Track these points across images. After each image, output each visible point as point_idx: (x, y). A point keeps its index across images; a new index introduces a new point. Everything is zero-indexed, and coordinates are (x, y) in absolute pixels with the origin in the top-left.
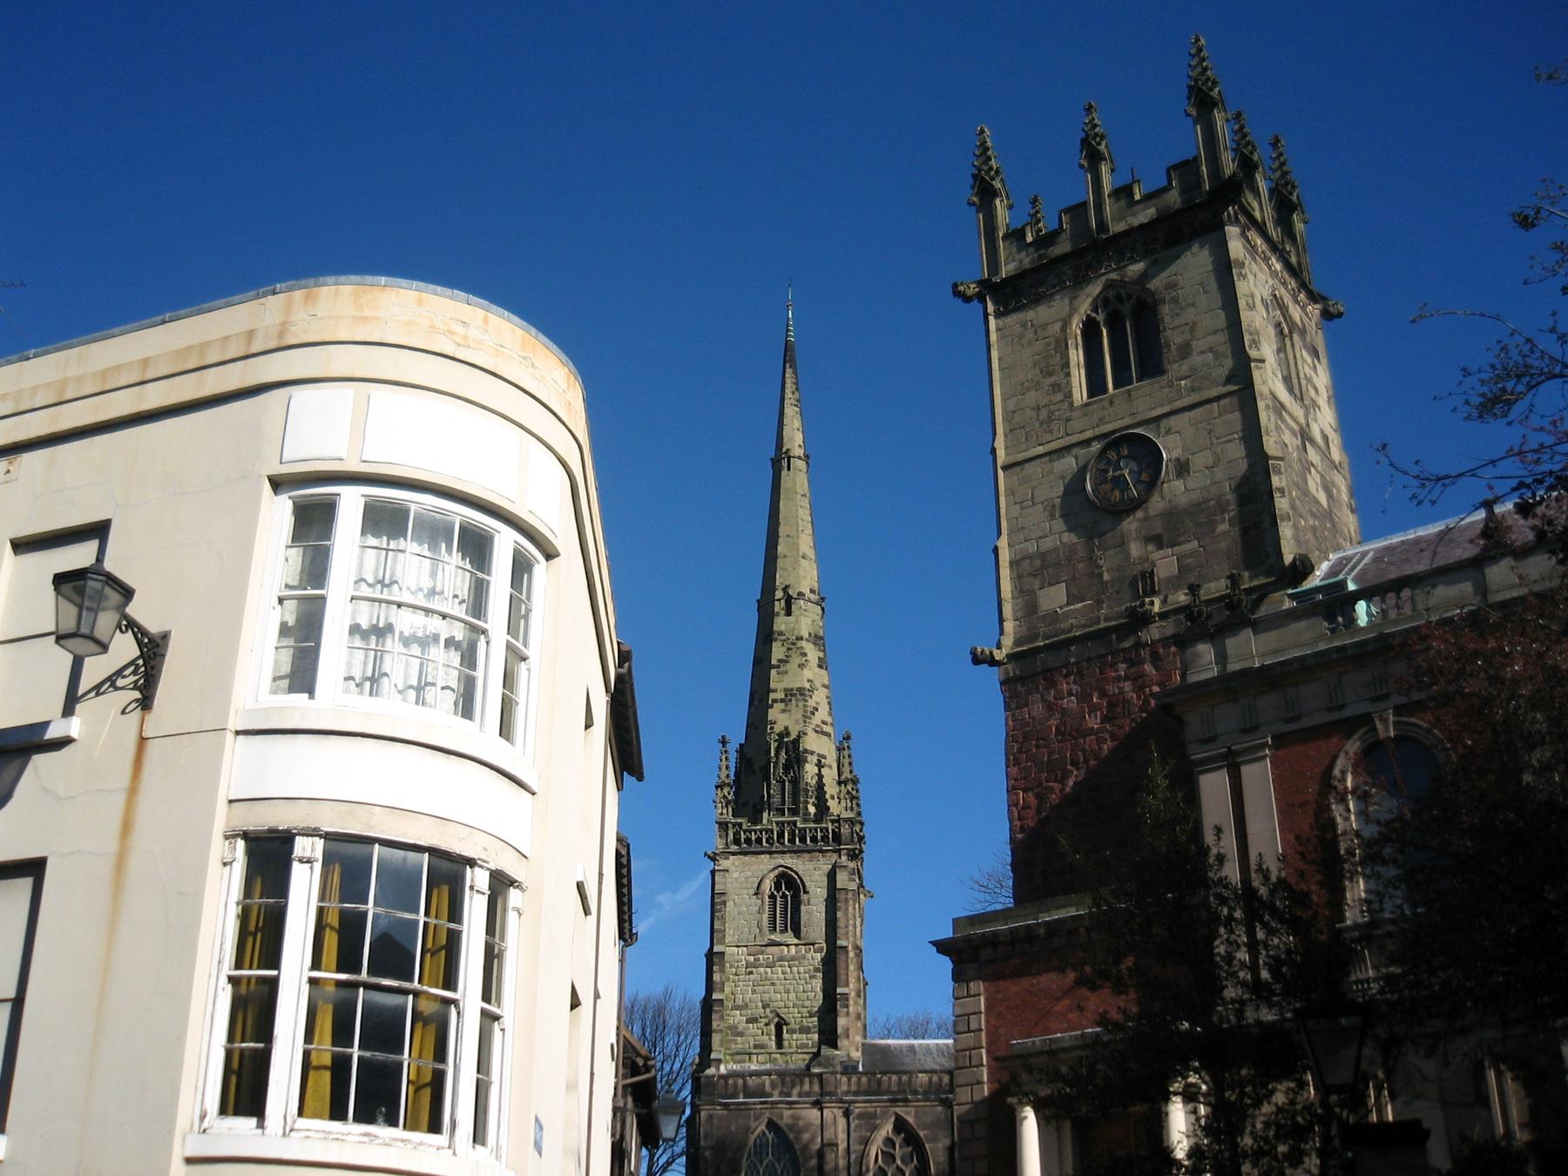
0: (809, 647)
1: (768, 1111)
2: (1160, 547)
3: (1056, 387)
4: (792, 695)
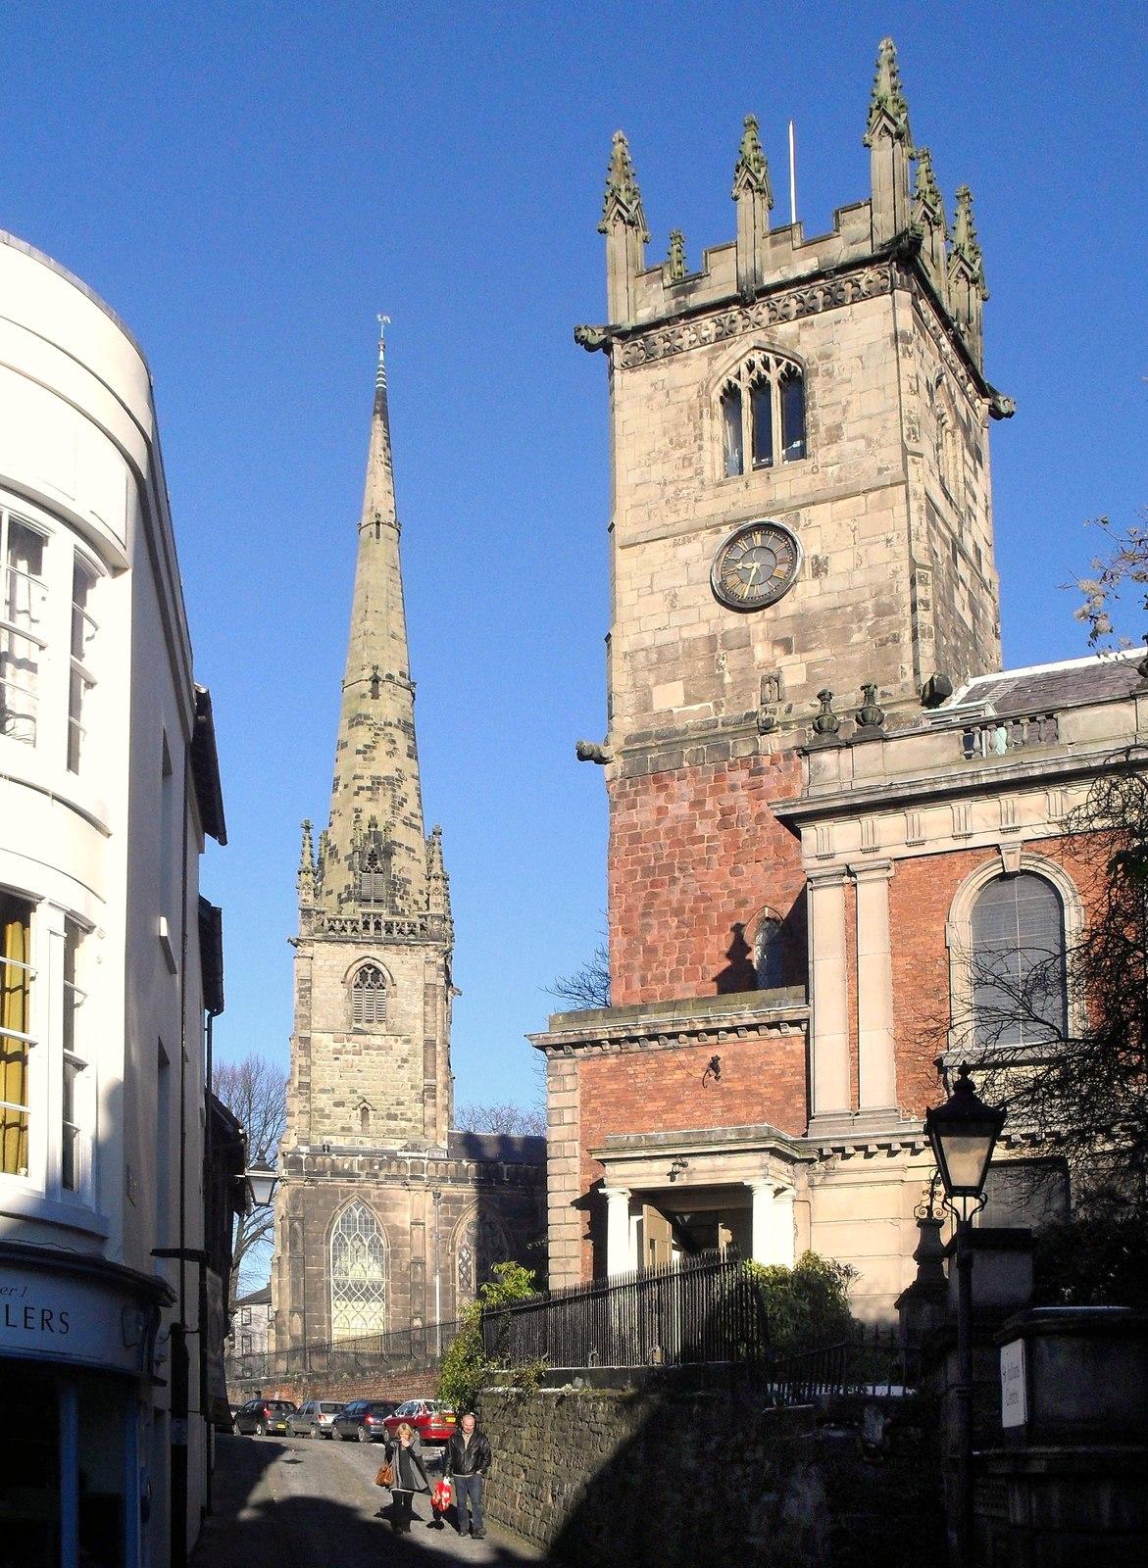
2: (788, 651)
3: (687, 461)
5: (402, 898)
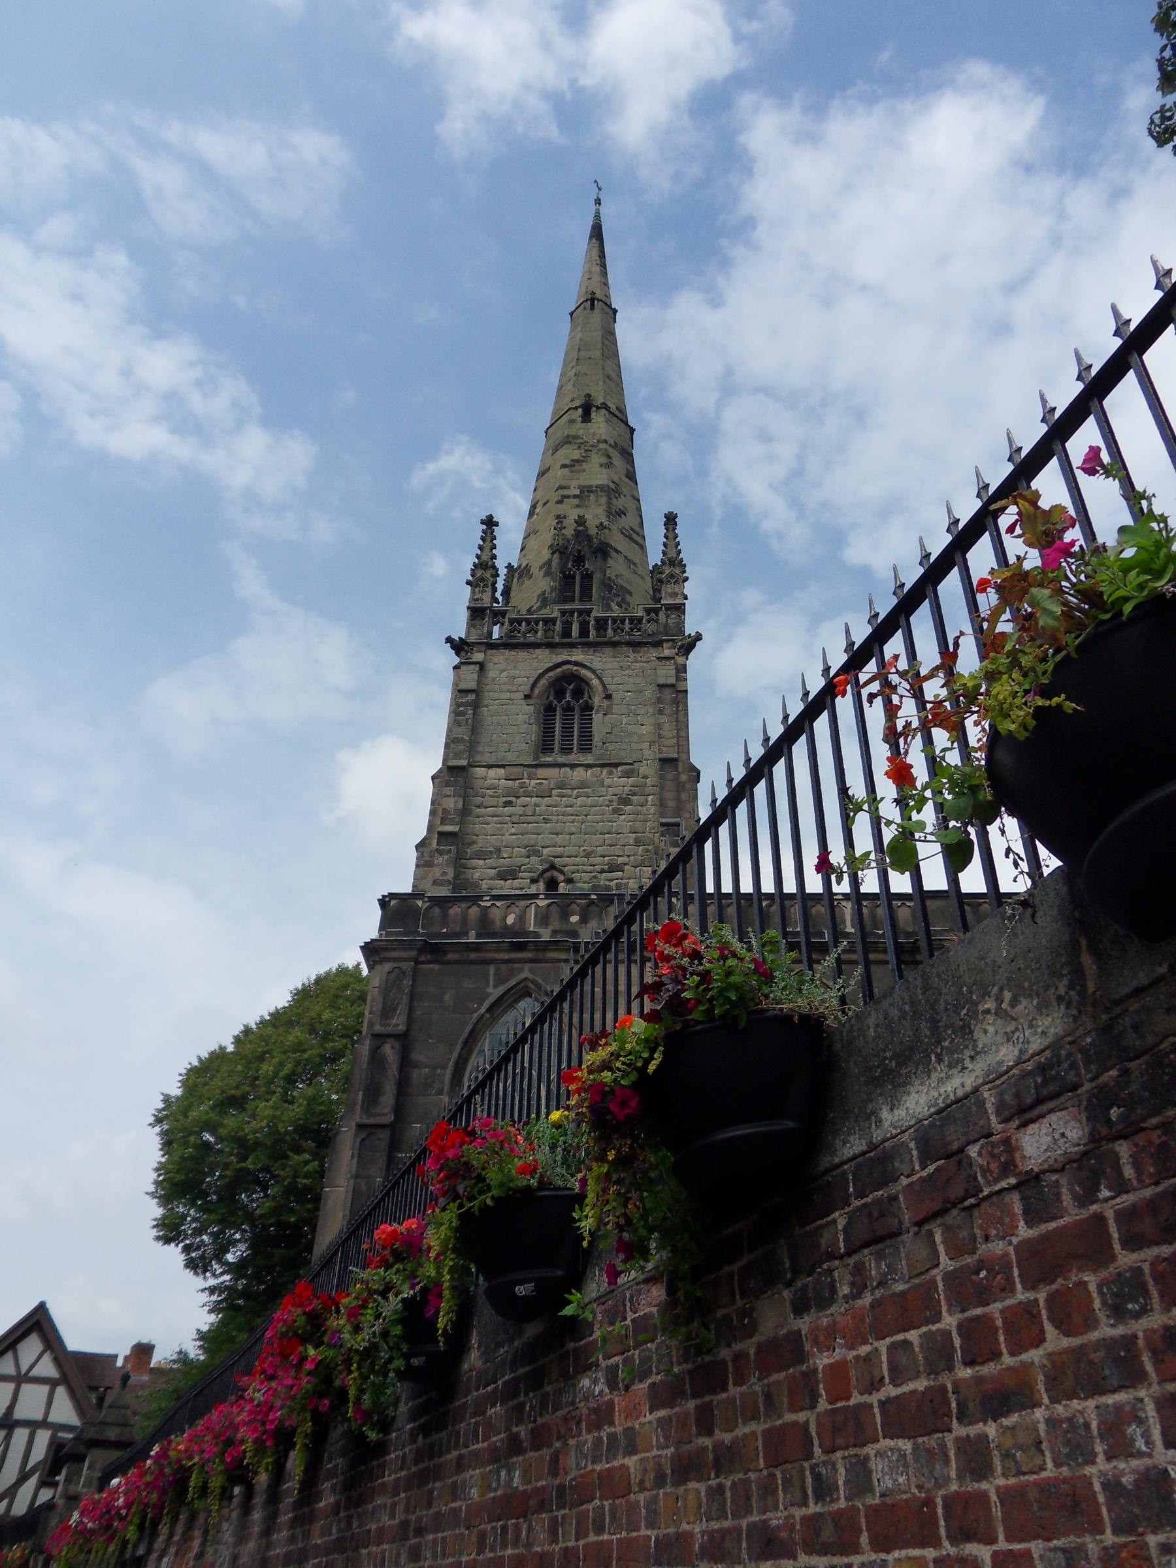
0: (615, 454)
1: (527, 966)
4: (591, 492)
5: (619, 605)
